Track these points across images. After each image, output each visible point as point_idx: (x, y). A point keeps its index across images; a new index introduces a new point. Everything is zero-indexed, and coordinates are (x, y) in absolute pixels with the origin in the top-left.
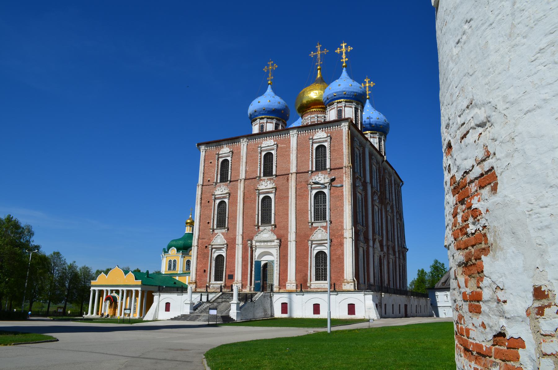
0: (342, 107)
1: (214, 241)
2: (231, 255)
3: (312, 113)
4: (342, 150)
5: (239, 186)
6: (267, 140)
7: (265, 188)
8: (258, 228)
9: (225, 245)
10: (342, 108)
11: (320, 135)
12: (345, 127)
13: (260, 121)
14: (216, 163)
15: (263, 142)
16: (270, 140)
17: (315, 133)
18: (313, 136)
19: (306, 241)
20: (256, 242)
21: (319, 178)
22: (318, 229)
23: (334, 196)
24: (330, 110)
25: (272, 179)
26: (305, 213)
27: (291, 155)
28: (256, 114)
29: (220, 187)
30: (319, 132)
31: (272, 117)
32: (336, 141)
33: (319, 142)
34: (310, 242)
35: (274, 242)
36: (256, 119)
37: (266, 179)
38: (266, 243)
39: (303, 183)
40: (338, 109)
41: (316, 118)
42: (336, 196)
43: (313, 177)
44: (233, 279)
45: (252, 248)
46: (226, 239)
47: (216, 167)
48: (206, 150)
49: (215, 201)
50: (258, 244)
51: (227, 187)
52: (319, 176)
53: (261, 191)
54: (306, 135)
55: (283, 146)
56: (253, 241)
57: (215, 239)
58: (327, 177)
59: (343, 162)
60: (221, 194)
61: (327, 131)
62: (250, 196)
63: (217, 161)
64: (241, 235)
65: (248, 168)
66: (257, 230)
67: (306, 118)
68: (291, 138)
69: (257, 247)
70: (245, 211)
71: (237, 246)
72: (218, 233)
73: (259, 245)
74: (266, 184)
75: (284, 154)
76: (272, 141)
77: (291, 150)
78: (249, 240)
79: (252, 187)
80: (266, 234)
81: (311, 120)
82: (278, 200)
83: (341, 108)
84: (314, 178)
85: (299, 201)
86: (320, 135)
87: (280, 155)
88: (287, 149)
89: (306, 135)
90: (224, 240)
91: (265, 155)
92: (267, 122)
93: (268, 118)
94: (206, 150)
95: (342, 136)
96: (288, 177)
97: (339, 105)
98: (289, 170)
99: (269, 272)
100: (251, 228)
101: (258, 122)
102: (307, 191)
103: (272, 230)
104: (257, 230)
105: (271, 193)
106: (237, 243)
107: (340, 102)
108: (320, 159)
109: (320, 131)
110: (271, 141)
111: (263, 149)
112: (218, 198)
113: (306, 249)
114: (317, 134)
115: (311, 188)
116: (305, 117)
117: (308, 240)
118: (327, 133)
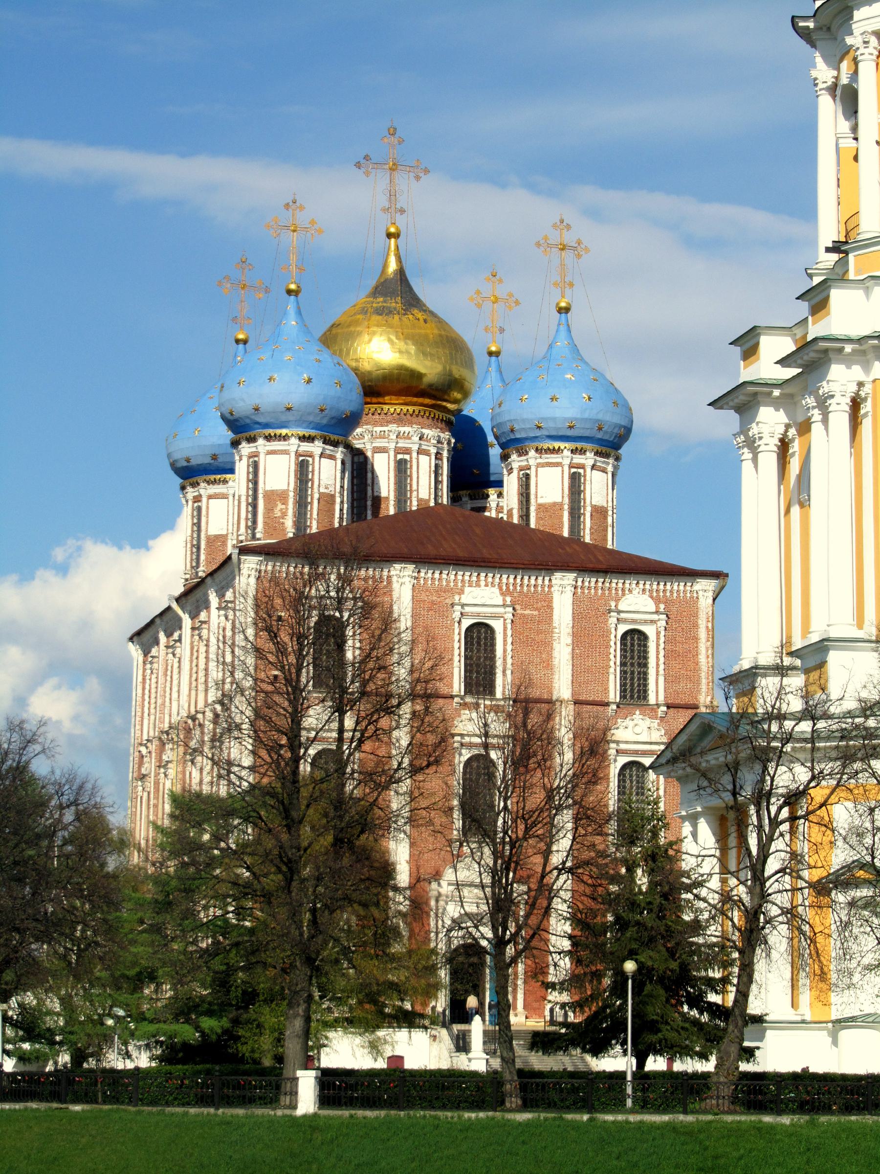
0: (583, 467)
3: (400, 419)
10: (585, 472)
12: (705, 594)
13: (299, 446)
17: (623, 595)
18: (617, 600)
24: (539, 465)
28: (290, 416)
31: (332, 439)
32: (680, 629)
33: (634, 621)
36: (285, 438)
40: (573, 470)
41: (416, 439)
48: (260, 572)
52: (635, 722)
54: (596, 593)
55: (527, 612)
56: (441, 881)
58: (656, 725)
59: (699, 691)
61: (655, 594)
67: (378, 429)
75: (534, 640)
76: (496, 590)
77: (557, 631)
81: (397, 443)
83: (581, 471)
87: (520, 639)
88: (543, 627)
89: (596, 593)
91: (467, 630)
92: (322, 455)
93: (326, 441)
94: (260, 572)
95: (696, 615)
97: (578, 459)
101: (293, 449)
102: (604, 756)
107: (582, 452)
108: (628, 669)
109: (638, 590)
114: (628, 596)
115: (617, 751)
116: (375, 424)
118: (657, 601)
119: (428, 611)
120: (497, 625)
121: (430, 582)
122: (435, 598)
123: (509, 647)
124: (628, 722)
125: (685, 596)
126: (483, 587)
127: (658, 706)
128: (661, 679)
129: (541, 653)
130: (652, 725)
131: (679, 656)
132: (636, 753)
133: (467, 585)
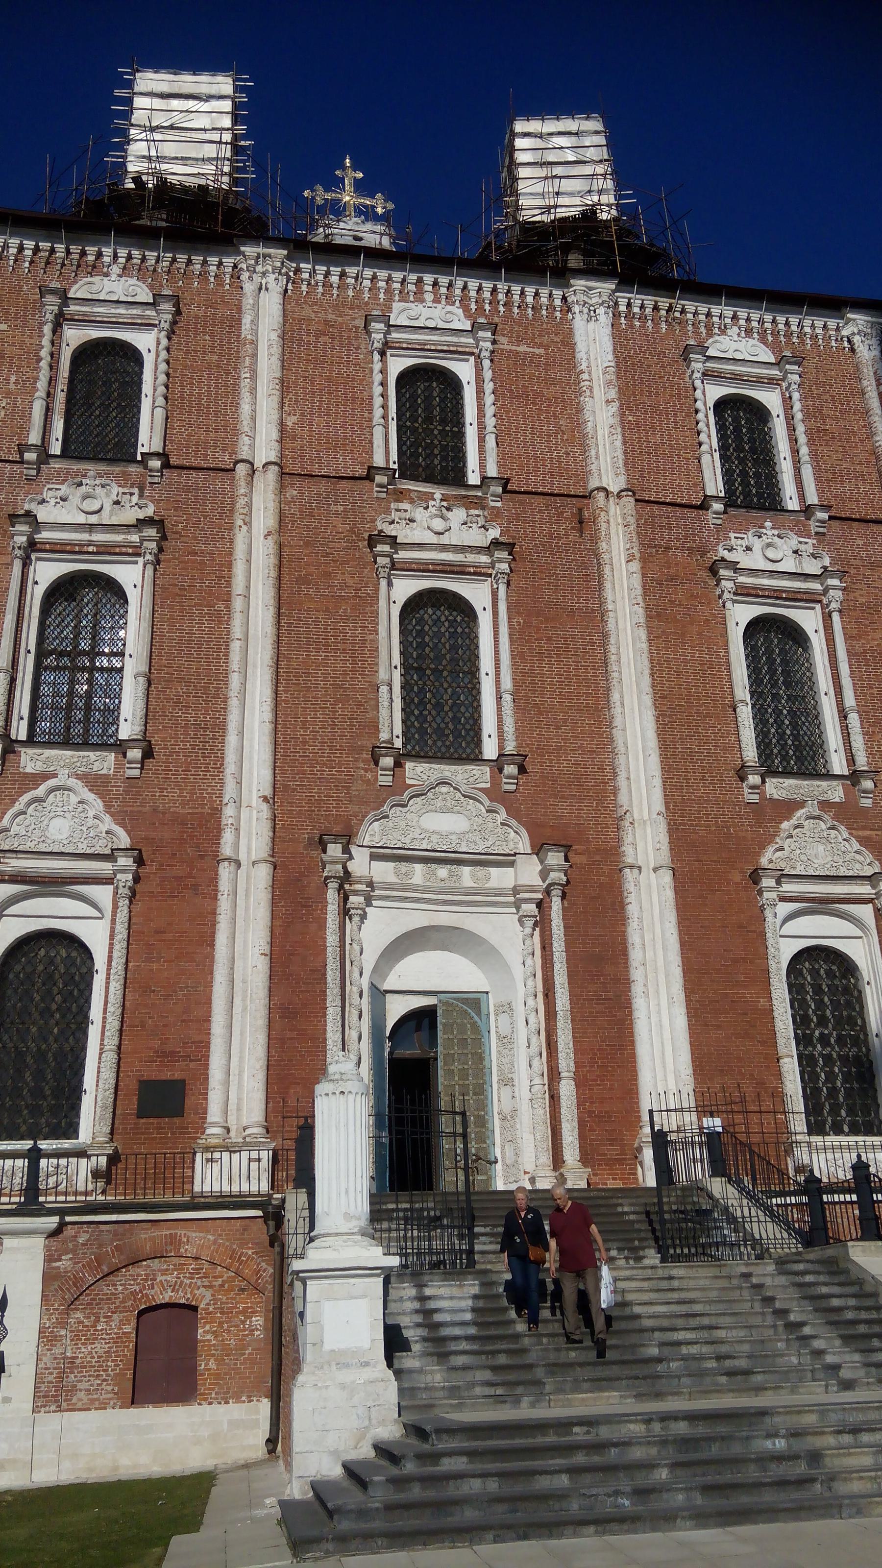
1: (15, 829)
2: (169, 936)
4: (862, 441)
5: (242, 501)
6: (422, 301)
7: (433, 539)
8: (398, 764)
9: (125, 861)
11: (735, 346)
14: (46, 342)
15: (397, 306)
16: (440, 306)
17: (710, 334)
19: (737, 877)
20: (374, 857)
21: (769, 545)
22: (800, 813)
23: (865, 652)
25: (480, 503)
26: (708, 715)
27: (588, 403)
29: (80, 484)
30: (729, 332)
33: (737, 378)
34: (767, 882)
35: (512, 864)
37: (438, 496)
38: (443, 872)
39: (681, 557)
42: (872, 650)
43: (732, 535)
44: (178, 1111)
45: (346, 898)
46: (119, 818)
47: (44, 364)
49: (26, 563)
50: (383, 872)
51: (136, 491)
53: (402, 555)
55: (522, 348)
56: (354, 849)
57: (25, 813)
60: (90, 528)
61: (770, 339)
62: (327, 575)
63: (47, 329)
64: (265, 799)
65: (294, 419)
66: (385, 780)
68: (579, 323)
69: (377, 892)
70: (289, 659)
71: (225, 871)
72: (45, 776)
73: (393, 879)
74: (438, 524)
75: (538, 394)
78: (336, 840)
79: (337, 522)
80: (449, 811)
82: (527, 624)
84: (740, 542)
85: (667, 649)
86: (735, 346)
87: (511, 391)
90: (108, 823)
91: (406, 378)
96: (580, 510)
98: (583, 475)
99: (450, 1073)
100: (340, 765)
103: (495, 794)
104: (385, 780)
105: (477, 573)
106: (227, 850)
109: (735, 329)
110: (449, 308)
111: (395, 335)
112: (59, 549)
113: (741, 926)
117: (755, 877)
119: (317, 336)
120: (464, 370)
121: (320, 289)
122: (330, 317)
123: (489, 399)
124: (750, 538)
125: (828, 346)
126: (430, 304)
127: (807, 510)
128: (807, 472)
129: (555, 417)
130: (802, 547)
131: (833, 438)
132: (776, 595)
133: (397, 298)
